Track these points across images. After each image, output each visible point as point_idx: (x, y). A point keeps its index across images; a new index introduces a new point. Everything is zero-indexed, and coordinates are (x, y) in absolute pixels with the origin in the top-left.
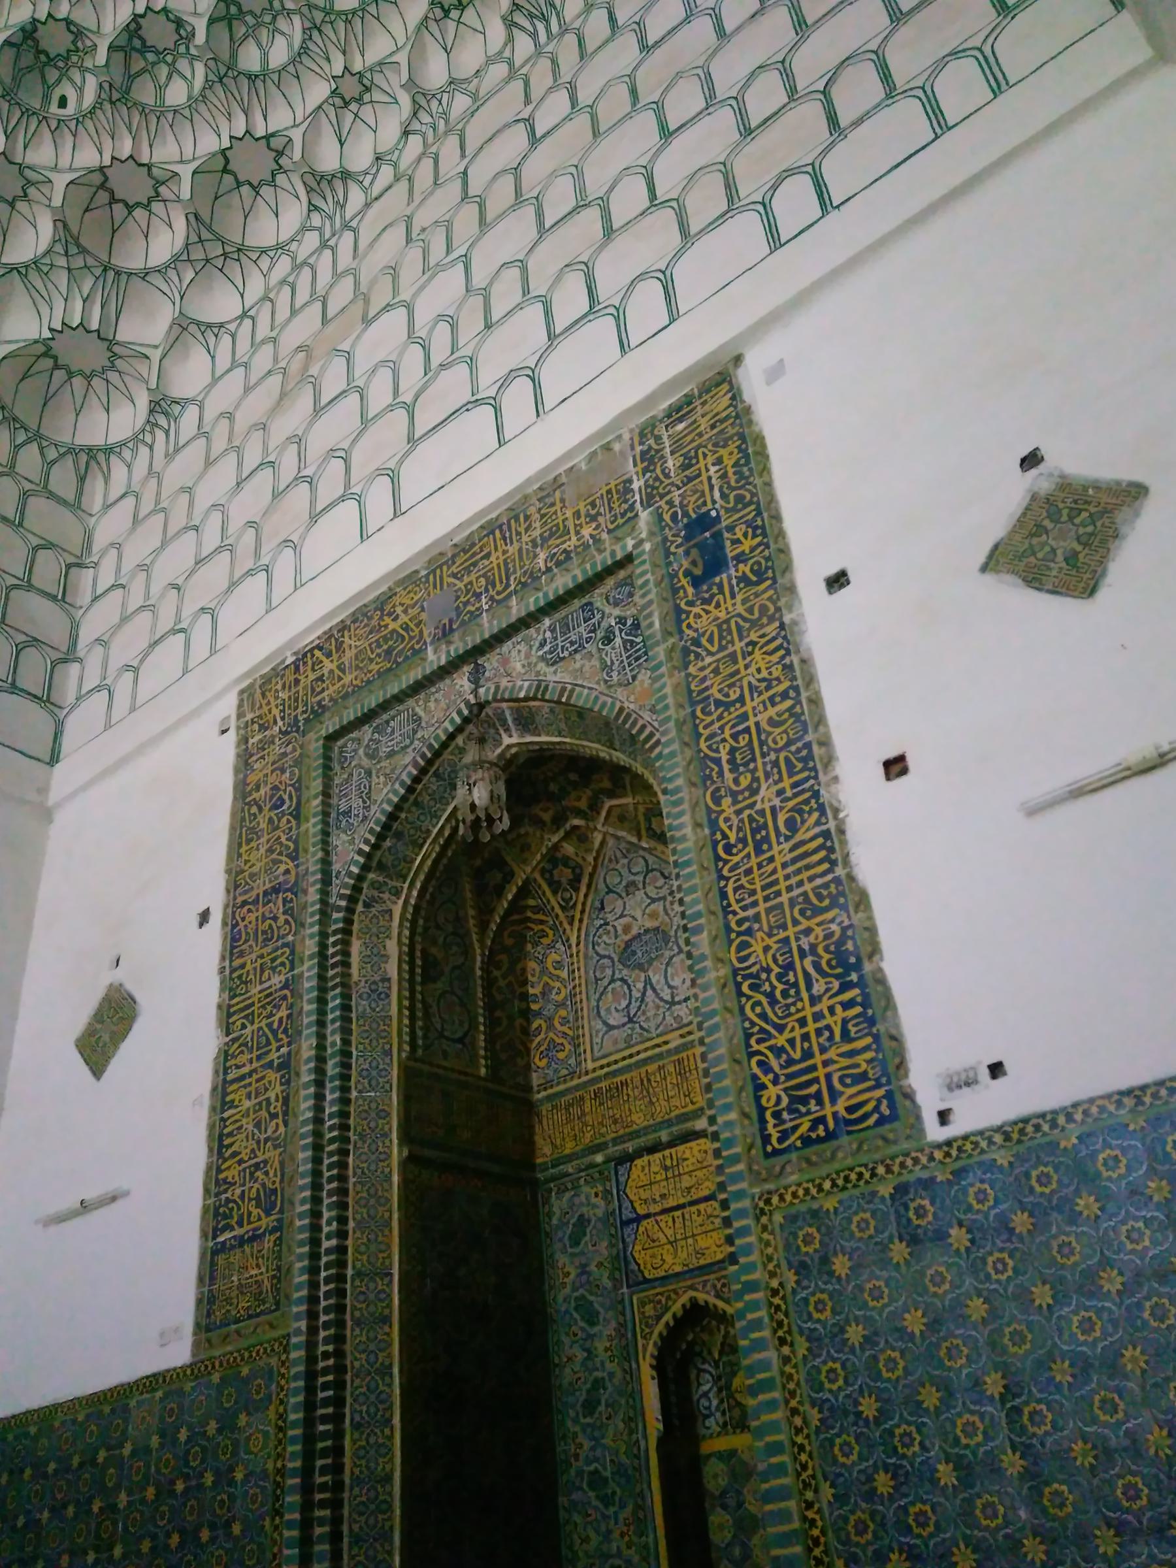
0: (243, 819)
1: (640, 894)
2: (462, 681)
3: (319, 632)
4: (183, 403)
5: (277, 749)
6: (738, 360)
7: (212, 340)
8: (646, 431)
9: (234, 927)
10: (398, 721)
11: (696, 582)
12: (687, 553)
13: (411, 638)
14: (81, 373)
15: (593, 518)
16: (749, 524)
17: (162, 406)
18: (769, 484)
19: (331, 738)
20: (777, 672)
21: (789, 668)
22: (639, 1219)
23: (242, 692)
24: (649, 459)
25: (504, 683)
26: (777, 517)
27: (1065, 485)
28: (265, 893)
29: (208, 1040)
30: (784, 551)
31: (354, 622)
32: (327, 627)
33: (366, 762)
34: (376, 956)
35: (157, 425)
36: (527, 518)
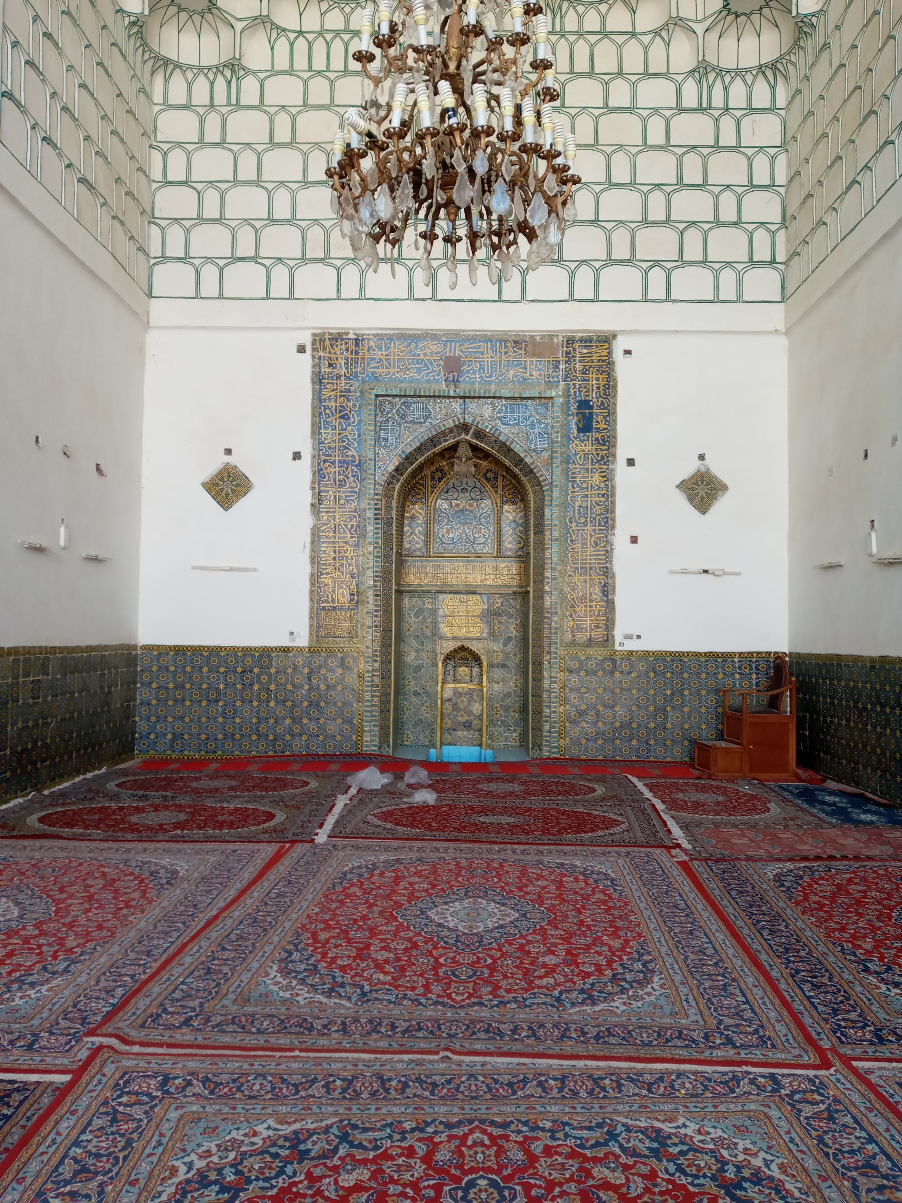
0: (320, 413)
1: (467, 494)
2: (456, 405)
3: (374, 332)
4: (248, 72)
5: (342, 384)
6: (615, 337)
7: (274, 35)
8: (570, 341)
9: (320, 470)
10: (416, 407)
11: (580, 430)
12: (578, 414)
13: (433, 371)
14: (180, 7)
15: (539, 370)
16: (605, 417)
17: (233, 68)
18: (615, 404)
19: (377, 396)
20: (602, 485)
21: (607, 486)
22: (447, 616)
23: (314, 335)
24: (569, 358)
25: (478, 419)
26: (615, 421)
27: (708, 471)
28: (340, 461)
29: (306, 521)
30: (615, 437)
31: (399, 339)
32: (380, 332)
33: (397, 417)
34: (389, 508)
35: (222, 73)
36: (506, 347)
